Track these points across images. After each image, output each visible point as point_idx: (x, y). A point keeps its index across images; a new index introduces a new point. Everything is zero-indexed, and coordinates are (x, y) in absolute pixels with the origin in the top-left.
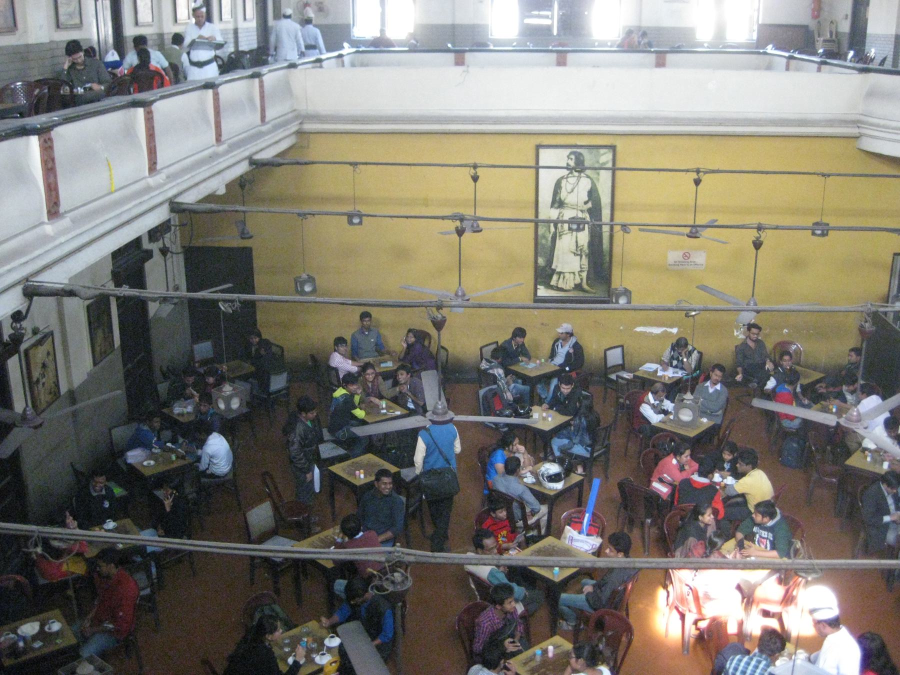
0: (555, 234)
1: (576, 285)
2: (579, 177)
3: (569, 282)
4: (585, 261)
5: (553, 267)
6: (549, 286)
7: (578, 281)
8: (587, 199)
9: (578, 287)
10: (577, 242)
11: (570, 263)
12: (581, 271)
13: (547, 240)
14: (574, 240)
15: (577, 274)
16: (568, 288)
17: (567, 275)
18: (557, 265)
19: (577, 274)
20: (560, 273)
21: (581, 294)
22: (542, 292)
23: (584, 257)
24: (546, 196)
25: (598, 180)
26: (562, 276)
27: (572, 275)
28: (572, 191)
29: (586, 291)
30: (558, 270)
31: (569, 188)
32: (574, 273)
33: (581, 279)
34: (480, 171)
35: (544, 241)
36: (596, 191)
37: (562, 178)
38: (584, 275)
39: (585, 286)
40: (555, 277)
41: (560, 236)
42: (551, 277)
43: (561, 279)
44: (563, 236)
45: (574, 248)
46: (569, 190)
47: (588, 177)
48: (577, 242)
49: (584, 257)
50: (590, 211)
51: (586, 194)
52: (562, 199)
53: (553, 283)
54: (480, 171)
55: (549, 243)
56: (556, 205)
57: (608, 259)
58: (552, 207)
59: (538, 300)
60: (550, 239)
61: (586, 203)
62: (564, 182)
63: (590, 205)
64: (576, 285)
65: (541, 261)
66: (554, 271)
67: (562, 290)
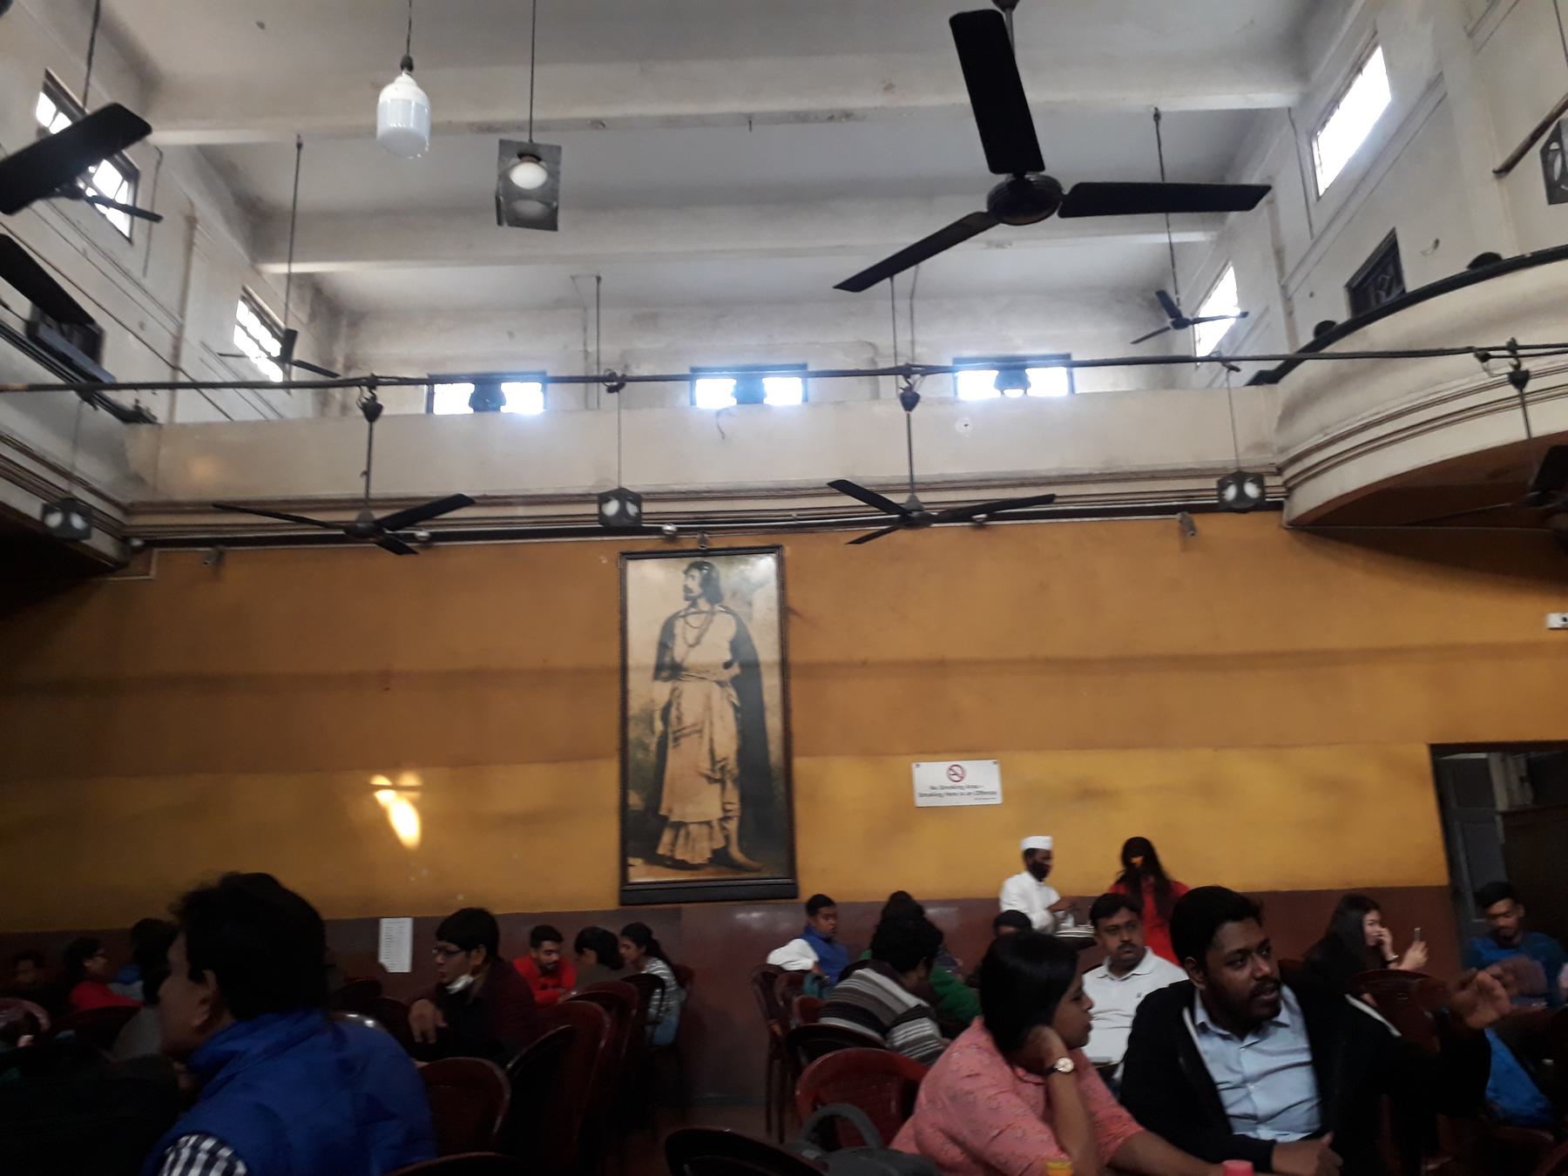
0: (664, 736)
1: (714, 852)
2: (712, 613)
3: (699, 851)
4: (733, 796)
5: (663, 812)
6: (653, 859)
7: (719, 843)
9: (720, 857)
11: (703, 808)
12: (725, 819)
13: (646, 748)
15: (715, 824)
16: (698, 861)
17: (692, 827)
20: (679, 825)
22: (641, 873)
23: (729, 785)
24: (642, 651)
25: (750, 618)
26: (682, 832)
27: (705, 829)
28: (698, 642)
29: (739, 867)
30: (674, 819)
31: (691, 635)
32: (708, 823)
33: (727, 838)
34: (384, 394)
35: (640, 755)
36: (749, 639)
37: (675, 616)
38: (732, 826)
39: (736, 853)
40: (667, 837)
41: (676, 739)
42: (657, 838)
43: (681, 841)
44: (683, 741)
45: (705, 765)
46: (691, 640)
47: (728, 611)
49: (729, 785)
50: (736, 682)
51: (726, 646)
52: (678, 659)
53: (661, 851)
54: (384, 394)
55: (652, 758)
56: (665, 674)
57: (782, 788)
58: (657, 676)
59: (630, 895)
60: (653, 747)
61: (727, 665)
62: (679, 625)
63: (735, 670)
64: (714, 852)
65: (635, 800)
66: (665, 819)
67: (682, 865)
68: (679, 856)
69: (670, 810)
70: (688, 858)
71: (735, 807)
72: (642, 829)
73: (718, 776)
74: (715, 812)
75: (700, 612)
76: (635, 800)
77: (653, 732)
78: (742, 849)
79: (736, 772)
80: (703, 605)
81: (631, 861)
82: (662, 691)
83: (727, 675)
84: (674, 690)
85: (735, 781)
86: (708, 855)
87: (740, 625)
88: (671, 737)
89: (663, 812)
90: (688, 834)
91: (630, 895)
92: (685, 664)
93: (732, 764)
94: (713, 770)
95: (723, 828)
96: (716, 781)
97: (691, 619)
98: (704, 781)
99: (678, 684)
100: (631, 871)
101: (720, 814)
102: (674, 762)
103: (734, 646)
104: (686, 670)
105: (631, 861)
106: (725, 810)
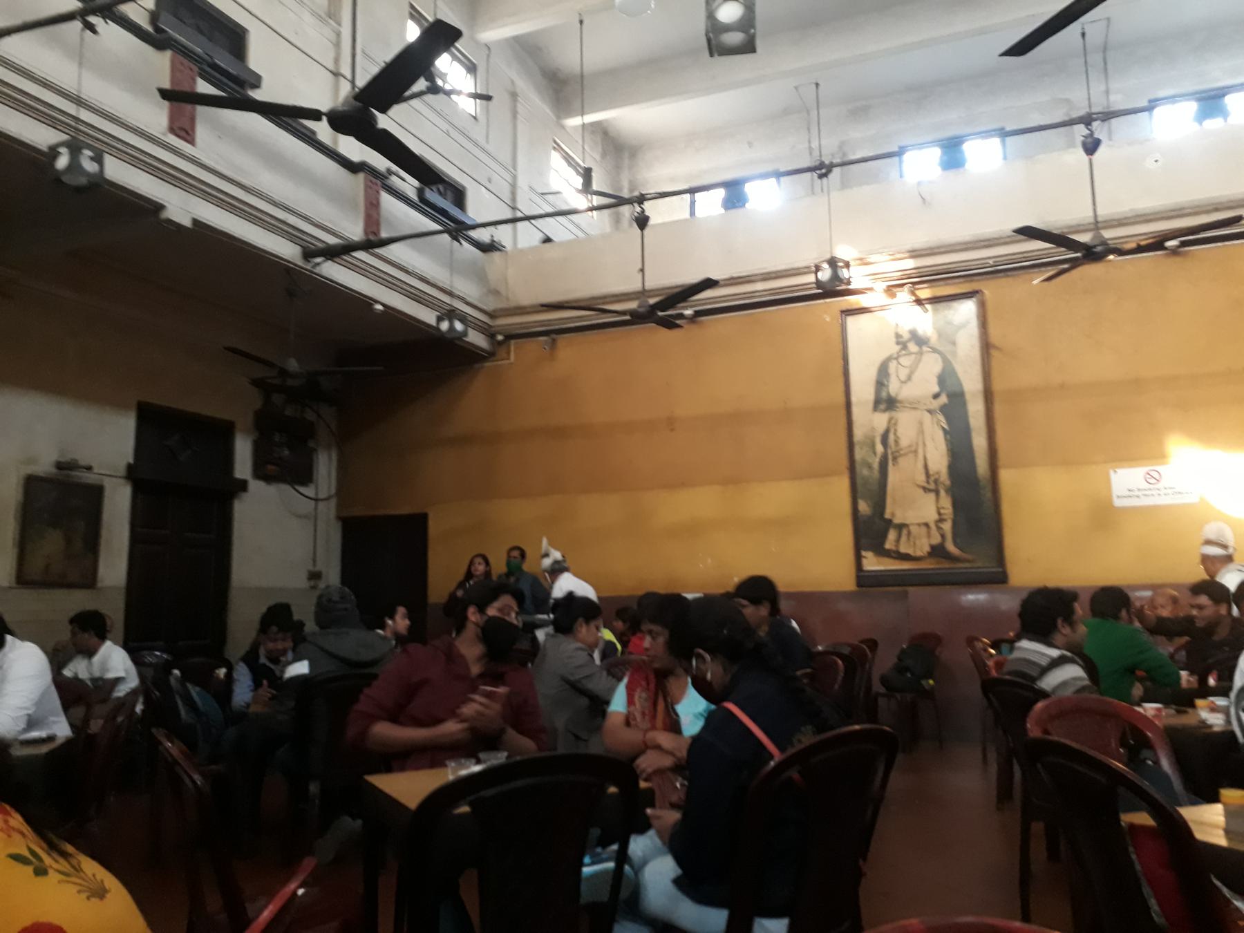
1: (933, 547)
2: (921, 353)
3: (921, 547)
4: (946, 503)
5: (887, 516)
6: (881, 552)
7: (936, 540)
8: (936, 389)
9: (938, 551)
10: (926, 467)
11: (921, 513)
13: (870, 467)
14: (920, 465)
15: (933, 526)
16: (919, 553)
17: (913, 529)
18: (896, 511)
19: (933, 526)
20: (900, 527)
21: (946, 565)
22: (872, 563)
23: (942, 493)
24: (863, 391)
25: (954, 354)
26: (905, 532)
27: (924, 529)
28: (909, 378)
30: (897, 521)
31: (903, 374)
32: (927, 525)
33: (943, 536)
35: (865, 472)
36: (953, 373)
37: (889, 359)
38: (947, 526)
39: (951, 547)
40: (892, 535)
41: (895, 459)
42: (884, 536)
43: (904, 538)
44: (901, 460)
45: (921, 478)
46: (903, 378)
48: (926, 467)
49: (942, 493)
50: (944, 409)
51: (935, 380)
52: (893, 393)
53: (888, 546)
56: (882, 407)
57: (989, 495)
59: (865, 580)
60: (876, 466)
61: (936, 396)
62: (892, 366)
63: (944, 399)
65: (863, 507)
66: (889, 522)
68: (903, 549)
69: (893, 515)
70: (910, 551)
71: (948, 509)
72: (871, 530)
73: (932, 486)
74: (931, 515)
75: (910, 354)
76: (863, 507)
77: (875, 453)
78: (956, 544)
79: (948, 483)
81: (864, 553)
82: (880, 421)
83: (936, 404)
84: (890, 419)
85: (947, 491)
86: (927, 549)
87: (946, 362)
88: (890, 457)
89: (887, 516)
90: (909, 533)
91: (865, 580)
92: (900, 398)
93: (944, 477)
94: (928, 482)
95: (939, 528)
96: (930, 490)
97: (902, 360)
98: (921, 491)
99: (894, 414)
100: (864, 561)
101: (936, 517)
102: (893, 477)
103: (942, 380)
104: (900, 402)
105: (864, 553)
106: (939, 514)
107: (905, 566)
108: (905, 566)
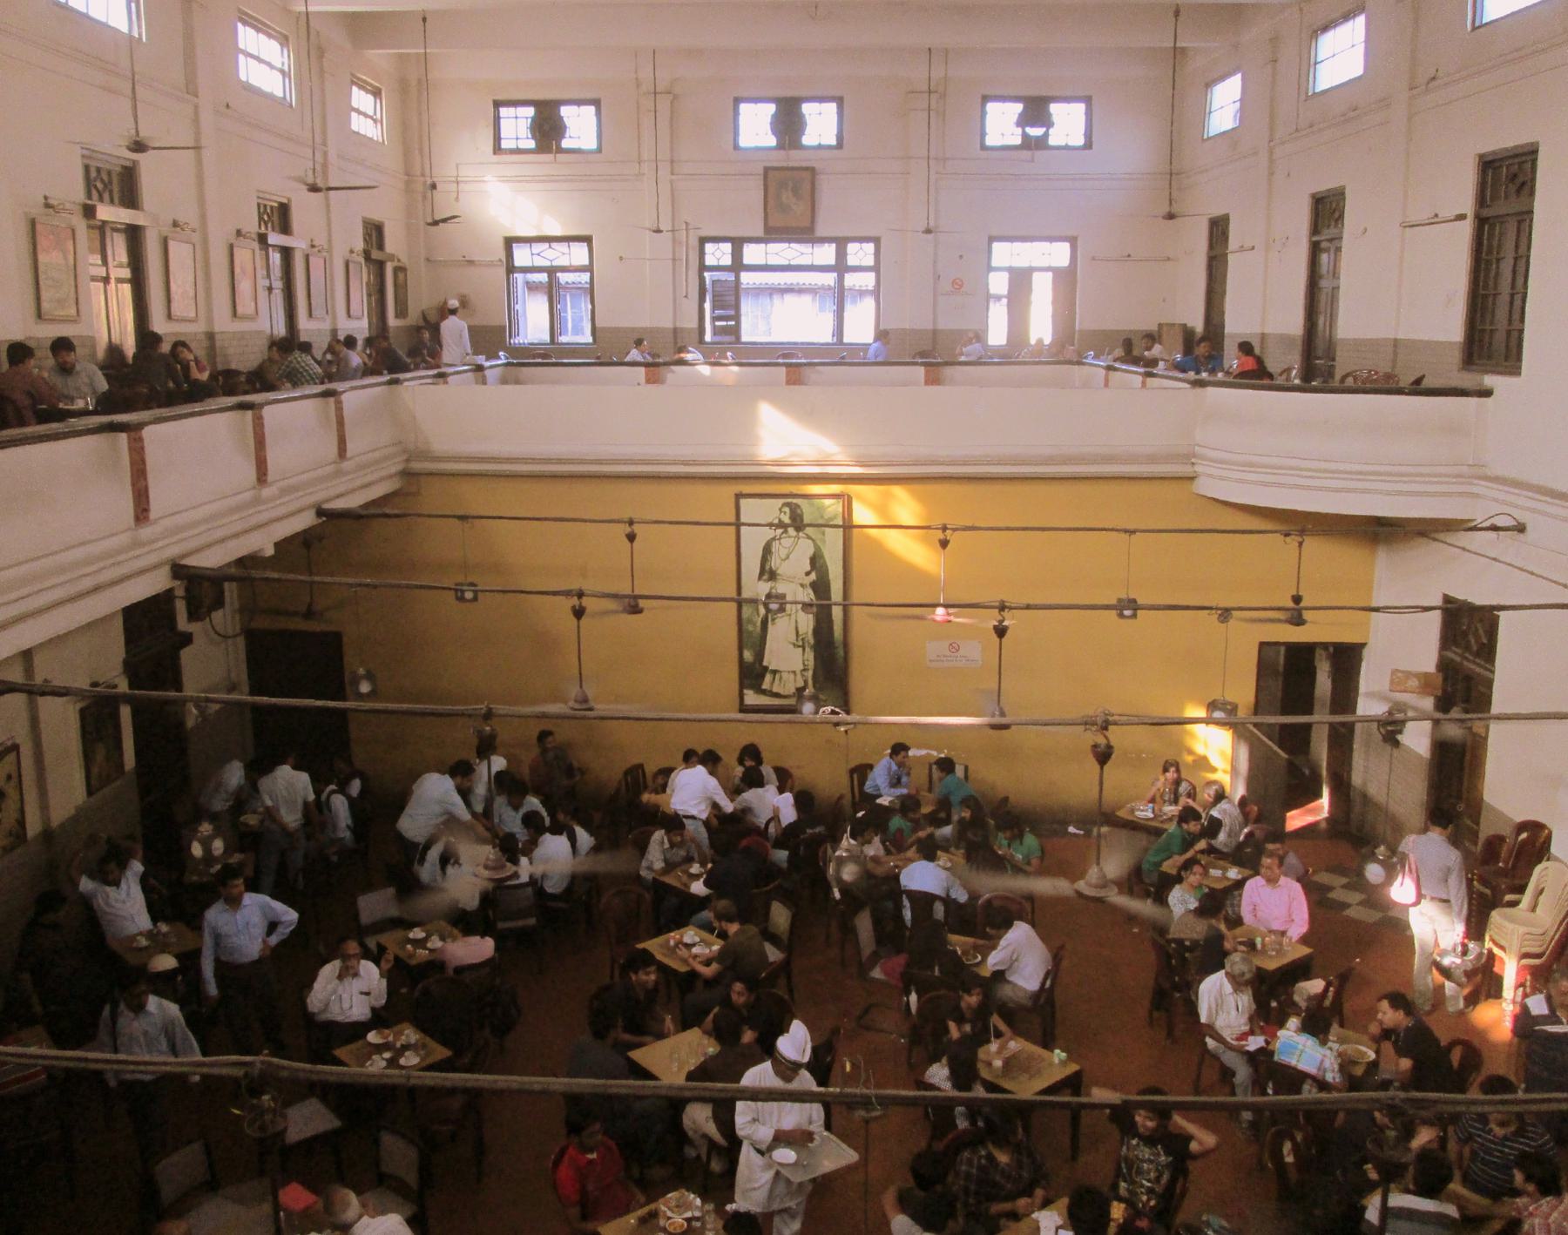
3: (790, 688)
4: (810, 655)
5: (765, 663)
7: (801, 684)
17: (785, 675)
18: (770, 660)
20: (775, 672)
22: (751, 698)
24: (751, 564)
34: (636, 528)
35: (750, 628)
36: (822, 557)
37: (774, 539)
38: (810, 673)
40: (768, 677)
42: (762, 677)
45: (793, 637)
47: (809, 537)
54: (636, 528)
55: (759, 629)
57: (841, 652)
58: (760, 578)
59: (744, 709)
61: (808, 574)
62: (775, 545)
63: (813, 576)
65: (748, 655)
66: (766, 668)
67: (777, 695)
70: (782, 692)
71: (811, 663)
80: (791, 531)
87: (816, 546)
89: (765, 663)
107: (776, 702)
108: (776, 702)
